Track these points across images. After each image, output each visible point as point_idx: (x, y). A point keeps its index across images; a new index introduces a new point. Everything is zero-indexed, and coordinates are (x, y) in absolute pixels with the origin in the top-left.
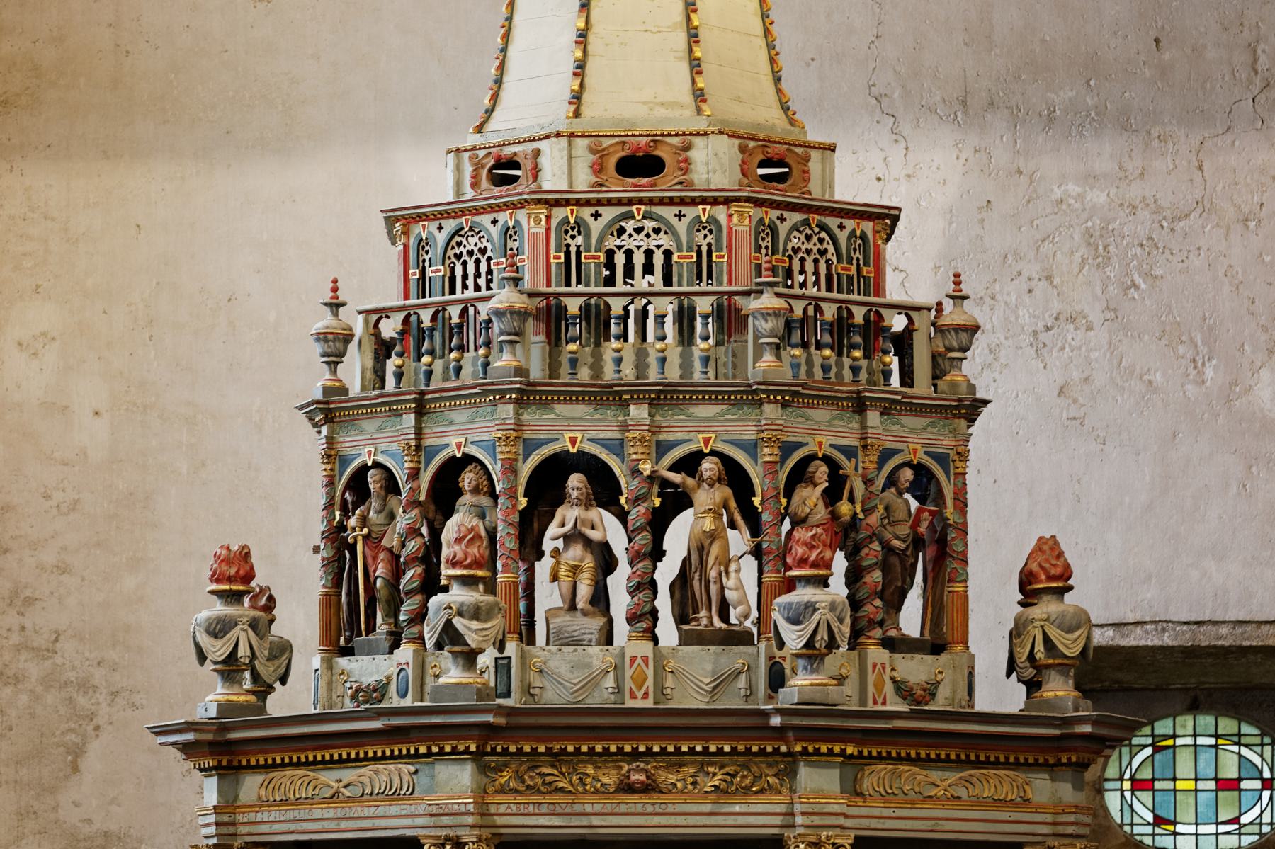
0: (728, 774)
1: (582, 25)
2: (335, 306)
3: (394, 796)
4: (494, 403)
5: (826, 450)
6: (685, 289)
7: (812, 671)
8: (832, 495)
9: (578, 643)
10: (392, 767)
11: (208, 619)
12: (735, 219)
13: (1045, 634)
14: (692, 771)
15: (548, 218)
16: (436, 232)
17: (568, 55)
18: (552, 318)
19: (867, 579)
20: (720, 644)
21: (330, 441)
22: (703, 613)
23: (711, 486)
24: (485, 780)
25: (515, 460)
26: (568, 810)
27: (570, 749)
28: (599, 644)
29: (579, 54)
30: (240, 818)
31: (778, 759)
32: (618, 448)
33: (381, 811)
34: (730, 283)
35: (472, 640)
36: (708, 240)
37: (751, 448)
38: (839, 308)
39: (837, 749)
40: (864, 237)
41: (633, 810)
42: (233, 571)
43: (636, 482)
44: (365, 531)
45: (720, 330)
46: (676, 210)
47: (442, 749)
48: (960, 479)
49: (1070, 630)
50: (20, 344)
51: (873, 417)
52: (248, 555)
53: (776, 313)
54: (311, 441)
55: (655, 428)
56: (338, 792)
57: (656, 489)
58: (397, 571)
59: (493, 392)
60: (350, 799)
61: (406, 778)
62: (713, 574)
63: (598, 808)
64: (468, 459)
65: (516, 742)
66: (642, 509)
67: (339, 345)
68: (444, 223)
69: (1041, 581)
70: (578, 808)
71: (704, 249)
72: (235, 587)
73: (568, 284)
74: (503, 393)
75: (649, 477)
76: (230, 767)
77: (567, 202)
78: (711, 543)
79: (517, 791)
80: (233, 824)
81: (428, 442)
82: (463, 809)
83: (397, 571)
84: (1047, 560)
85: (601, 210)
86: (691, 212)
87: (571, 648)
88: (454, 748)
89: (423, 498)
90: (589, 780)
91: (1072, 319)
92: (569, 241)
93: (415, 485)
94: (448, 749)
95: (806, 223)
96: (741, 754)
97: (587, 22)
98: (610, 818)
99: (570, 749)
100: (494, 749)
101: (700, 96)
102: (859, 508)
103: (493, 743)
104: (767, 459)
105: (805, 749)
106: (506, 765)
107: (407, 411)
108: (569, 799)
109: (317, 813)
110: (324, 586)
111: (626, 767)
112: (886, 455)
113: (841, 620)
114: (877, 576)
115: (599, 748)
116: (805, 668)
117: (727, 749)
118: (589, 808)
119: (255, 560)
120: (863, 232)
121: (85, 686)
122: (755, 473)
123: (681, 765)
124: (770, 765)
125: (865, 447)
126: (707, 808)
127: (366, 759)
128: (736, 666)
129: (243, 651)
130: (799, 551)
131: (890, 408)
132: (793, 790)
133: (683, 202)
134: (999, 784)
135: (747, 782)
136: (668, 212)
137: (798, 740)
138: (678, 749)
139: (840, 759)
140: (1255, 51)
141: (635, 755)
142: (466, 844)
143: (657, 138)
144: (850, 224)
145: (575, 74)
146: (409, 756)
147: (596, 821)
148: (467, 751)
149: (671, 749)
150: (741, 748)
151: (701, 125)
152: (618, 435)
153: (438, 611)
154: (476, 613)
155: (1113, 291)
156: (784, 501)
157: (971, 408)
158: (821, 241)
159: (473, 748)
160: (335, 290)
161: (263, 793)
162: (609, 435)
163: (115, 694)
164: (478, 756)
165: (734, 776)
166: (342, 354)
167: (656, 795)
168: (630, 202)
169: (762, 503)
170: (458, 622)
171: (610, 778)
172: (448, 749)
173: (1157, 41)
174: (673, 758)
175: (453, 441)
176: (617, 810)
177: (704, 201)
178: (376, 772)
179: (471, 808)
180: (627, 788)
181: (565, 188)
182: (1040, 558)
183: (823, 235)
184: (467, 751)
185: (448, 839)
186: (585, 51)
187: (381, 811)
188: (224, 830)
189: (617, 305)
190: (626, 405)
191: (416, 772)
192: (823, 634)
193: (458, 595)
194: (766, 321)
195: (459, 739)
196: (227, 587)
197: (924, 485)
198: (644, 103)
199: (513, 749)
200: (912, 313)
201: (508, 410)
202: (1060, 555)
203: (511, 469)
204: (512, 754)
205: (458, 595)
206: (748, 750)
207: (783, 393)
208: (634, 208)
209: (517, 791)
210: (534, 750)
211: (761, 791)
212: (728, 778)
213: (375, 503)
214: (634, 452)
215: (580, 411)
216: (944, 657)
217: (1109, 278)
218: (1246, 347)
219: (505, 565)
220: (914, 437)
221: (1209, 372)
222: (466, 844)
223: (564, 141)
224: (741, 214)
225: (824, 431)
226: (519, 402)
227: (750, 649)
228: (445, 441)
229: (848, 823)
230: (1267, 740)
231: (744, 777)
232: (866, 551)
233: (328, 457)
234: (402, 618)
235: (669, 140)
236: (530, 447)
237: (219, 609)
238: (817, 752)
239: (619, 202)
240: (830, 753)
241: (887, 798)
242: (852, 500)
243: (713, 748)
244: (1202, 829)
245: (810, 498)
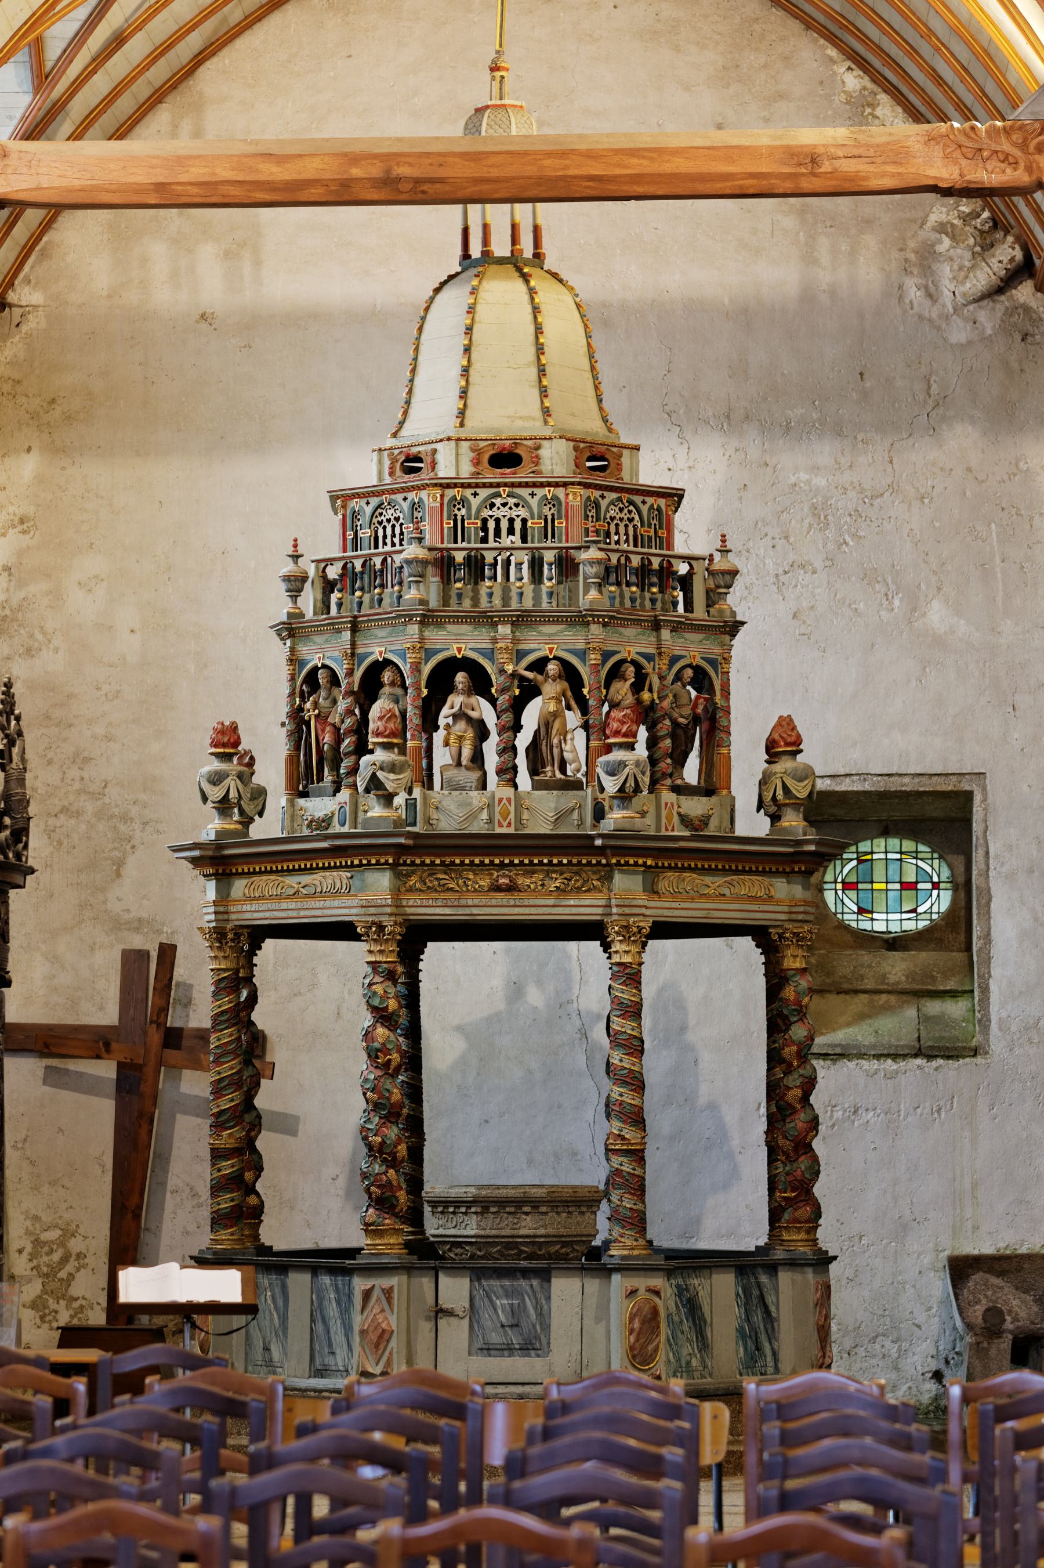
1: (465, 363)
2: (296, 557)
3: (336, 894)
4: (405, 624)
5: (633, 656)
6: (536, 545)
7: (624, 808)
8: (638, 687)
9: (463, 789)
10: (335, 874)
11: (209, 772)
12: (571, 497)
13: (783, 782)
14: (541, 877)
15: (442, 496)
16: (365, 506)
17: (456, 383)
18: (444, 565)
19: (661, 745)
20: (560, 790)
21: (292, 650)
22: (549, 768)
23: (554, 680)
24: (399, 883)
25: (420, 663)
26: (456, 903)
27: (458, 861)
28: (477, 789)
29: (463, 383)
30: (232, 909)
31: (600, 868)
32: (490, 655)
33: (328, 904)
35: (390, 787)
36: (552, 511)
37: (582, 655)
38: (642, 559)
39: (640, 862)
40: (659, 509)
42: (226, 739)
43: (502, 678)
44: (317, 711)
45: (560, 574)
46: (530, 490)
47: (369, 861)
48: (725, 676)
49: (801, 780)
50: (80, 584)
51: (665, 634)
52: (236, 728)
53: (599, 562)
54: (280, 650)
55: (515, 641)
56: (298, 891)
57: (516, 683)
58: (338, 740)
59: (404, 616)
60: (307, 896)
61: (345, 881)
62: (555, 741)
63: (476, 902)
64: (387, 663)
65: (420, 857)
67: (299, 584)
68: (370, 499)
69: (781, 746)
70: (463, 902)
71: (549, 518)
72: (227, 751)
73: (456, 542)
74: (411, 617)
75: (511, 675)
76: (224, 874)
77: (455, 485)
79: (421, 890)
80: (227, 913)
81: (359, 651)
83: (338, 740)
84: (785, 732)
85: (478, 490)
86: (540, 492)
87: (458, 792)
88: (378, 861)
89: (356, 689)
90: (470, 883)
91: (803, 567)
92: (456, 512)
93: (351, 680)
94: (373, 861)
95: (620, 499)
96: (575, 865)
97: (469, 361)
99: (458, 861)
100: (405, 862)
101: (546, 412)
102: (655, 696)
103: (404, 858)
104: (593, 662)
105: (619, 861)
106: (413, 872)
107: (345, 629)
108: (456, 896)
109: (284, 906)
110: (289, 750)
111: (496, 874)
112: (674, 659)
113: (643, 773)
114: (668, 742)
115: (477, 861)
116: (619, 806)
117: (565, 861)
118: (470, 902)
119: (240, 732)
120: (659, 506)
121: (125, 818)
122: (584, 671)
123: (534, 873)
124: (594, 873)
125: (660, 654)
126: (551, 902)
127: (318, 868)
128: (571, 805)
129: (233, 794)
130: (615, 725)
131: (677, 627)
132: (610, 890)
133: (534, 485)
134: (752, 885)
135: (579, 884)
136: (524, 492)
137: (614, 855)
138: (531, 862)
139: (643, 869)
140: (929, 381)
141: (502, 865)
143: (517, 442)
144: (650, 500)
145: (460, 397)
146: (347, 866)
147: (475, 911)
148: (386, 863)
149: (526, 861)
150: (575, 861)
151: (547, 432)
152: (490, 646)
153: (366, 767)
154: (393, 768)
155: (831, 546)
156: (604, 691)
157: (733, 627)
158: (630, 512)
159: (391, 861)
160: (295, 546)
161: (247, 891)
162: (484, 646)
163: (146, 824)
164: (394, 867)
165: (570, 880)
166: (300, 590)
167: (516, 893)
168: (498, 485)
169: (589, 692)
170: (380, 774)
171: (485, 882)
172: (373, 861)
173: (861, 374)
175: (377, 650)
177: (549, 484)
178: (324, 877)
179: (389, 902)
180: (497, 888)
181: (454, 475)
182: (780, 730)
183: (631, 508)
184: (386, 863)
185: (374, 923)
186: (467, 381)
187: (328, 904)
188: (220, 917)
189: (489, 556)
190: (495, 625)
191: (352, 877)
192: (631, 783)
193: (380, 756)
195: (381, 854)
196: (222, 750)
197: (701, 679)
198: (508, 417)
199: (418, 861)
200: (692, 562)
201: (414, 629)
202: (794, 728)
203: (416, 669)
204: (417, 865)
205: (380, 756)
206: (580, 862)
207: (603, 616)
208: (501, 489)
209: (421, 890)
210: (433, 862)
211: (589, 890)
212: (566, 882)
213: (323, 693)
214: (502, 657)
215: (465, 629)
216: (714, 799)
217: (828, 537)
218: (922, 585)
219: (413, 735)
220: (693, 648)
221: (897, 602)
223: (453, 443)
224: (575, 494)
225: (633, 643)
226: (421, 623)
227: (580, 793)
228: (371, 650)
229: (648, 912)
230: (936, 855)
231: (576, 881)
232: (660, 725)
233: (291, 661)
234: (342, 771)
235: (525, 442)
236: (430, 654)
237: (216, 765)
238: (627, 864)
239: (491, 485)
240: (636, 864)
241: (675, 895)
242: (651, 690)
243: (555, 861)
244: (891, 916)
245: (622, 689)
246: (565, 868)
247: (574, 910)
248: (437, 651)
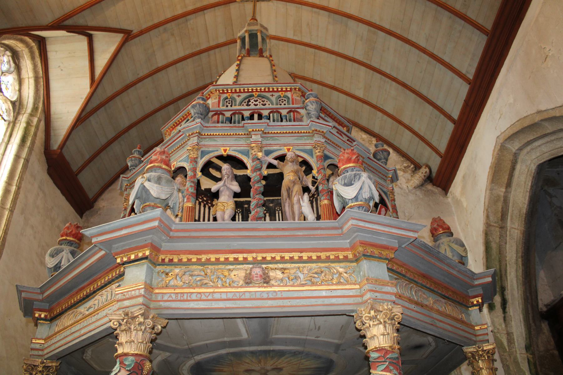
0: (316, 273)
25: (197, 158)
26: (210, 297)
32: (247, 154)
34: (293, 104)
41: (254, 297)
43: (255, 163)
66: (258, 173)
78: (294, 186)
82: (137, 294)
85: (240, 94)
98: (238, 302)
100: (163, 260)
104: (318, 154)
109: (73, 330)
122: (312, 161)
142: (137, 316)
162: (242, 148)
170: (147, 184)
174: (281, 266)
176: (243, 297)
185: (127, 314)
194: (312, 105)
201: (194, 140)
222: (137, 316)
246: (314, 265)
247: (327, 301)
248: (209, 152)
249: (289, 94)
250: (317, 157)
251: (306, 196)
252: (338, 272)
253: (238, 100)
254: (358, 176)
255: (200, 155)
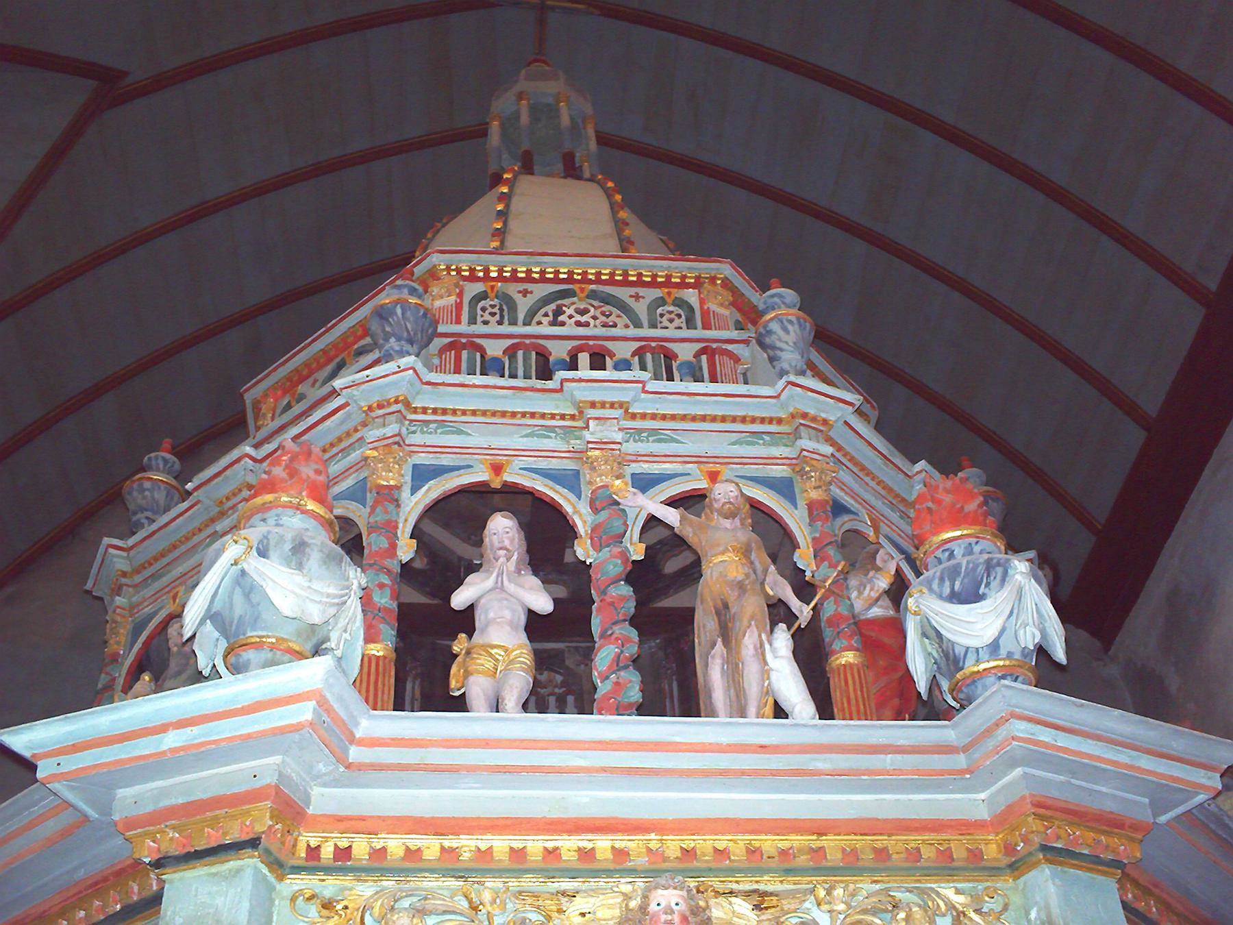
32: (570, 481)
100: (313, 852)
122: (795, 519)
152: (570, 465)
249: (691, 296)
250: (811, 506)
251: (782, 640)
252: (951, 906)
253: (523, 305)
254: (999, 570)
255: (408, 478)
